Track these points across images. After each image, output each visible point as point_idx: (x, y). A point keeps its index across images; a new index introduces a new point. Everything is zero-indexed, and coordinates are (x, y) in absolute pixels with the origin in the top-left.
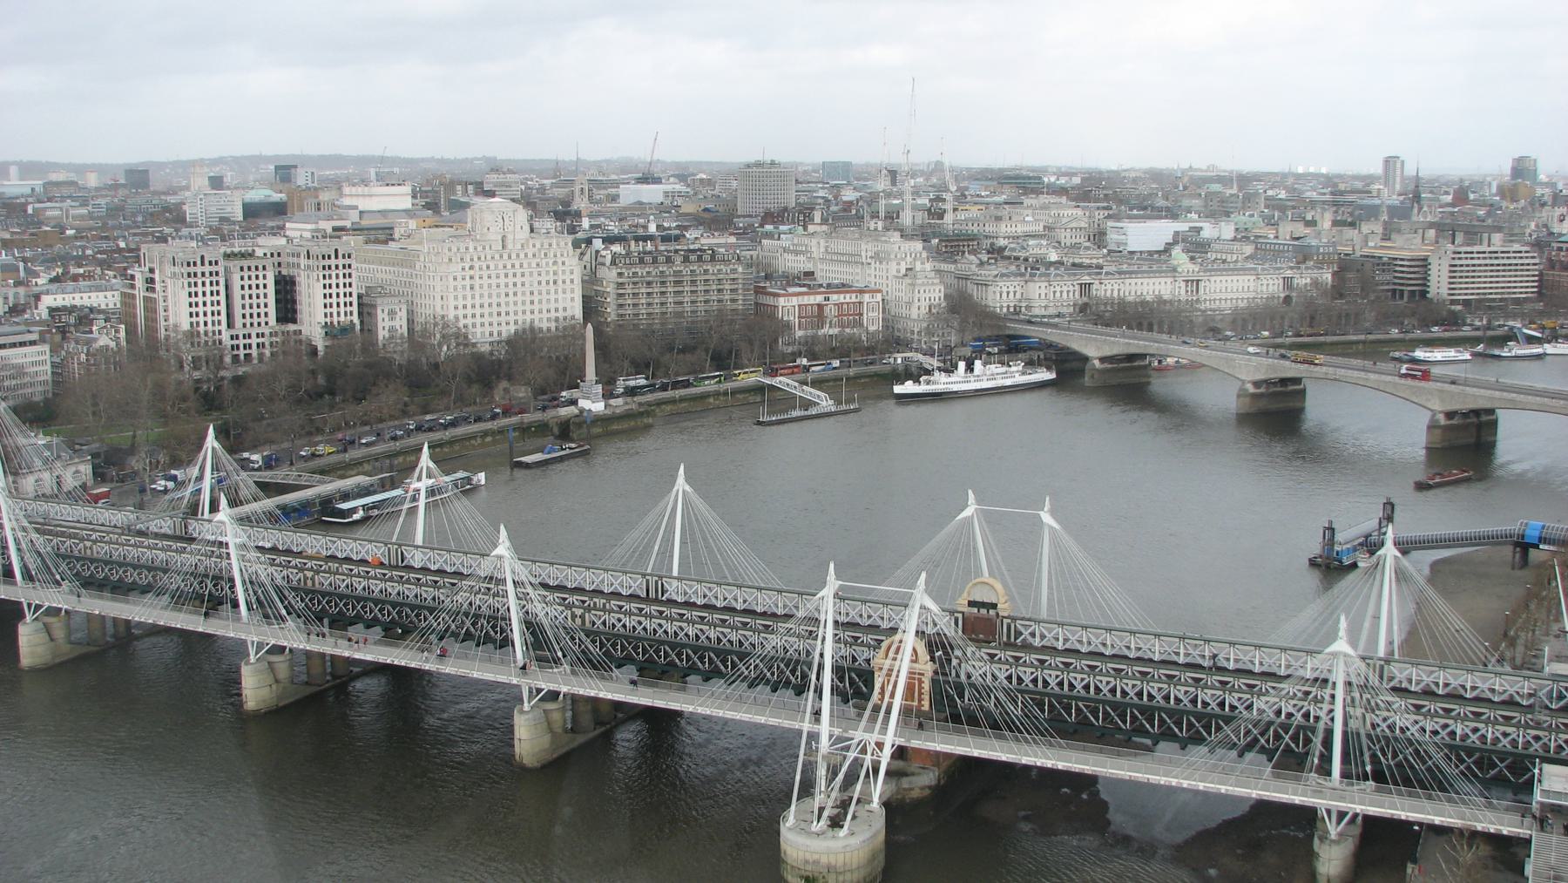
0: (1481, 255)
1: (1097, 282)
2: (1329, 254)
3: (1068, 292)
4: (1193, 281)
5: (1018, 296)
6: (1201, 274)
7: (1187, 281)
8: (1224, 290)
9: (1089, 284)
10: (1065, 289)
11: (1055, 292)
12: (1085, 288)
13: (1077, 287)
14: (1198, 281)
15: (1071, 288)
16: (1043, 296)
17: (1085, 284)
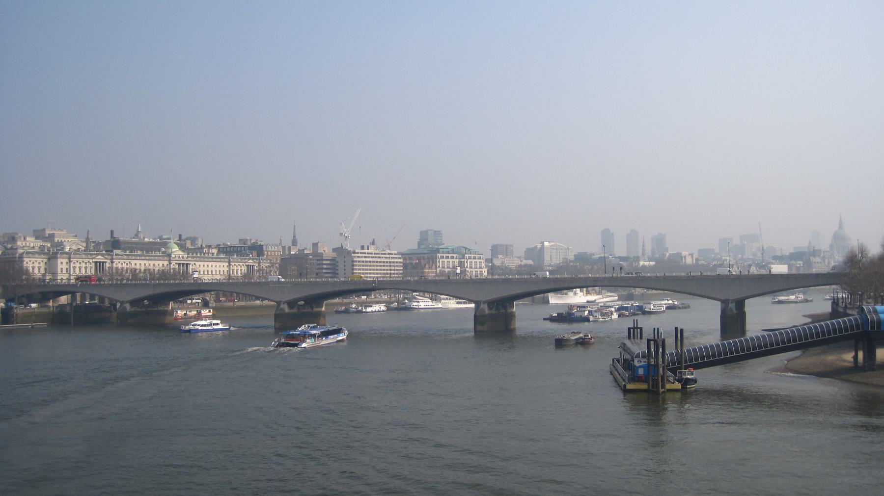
0: (370, 255)
1: (109, 261)
2: (275, 252)
3: (86, 268)
4: (183, 264)
5: (43, 271)
6: (189, 259)
7: (179, 264)
8: (206, 272)
9: (103, 262)
10: (83, 265)
11: (74, 268)
12: (99, 265)
13: (93, 265)
14: (187, 264)
15: (88, 265)
16: (64, 271)
17: (100, 262)
